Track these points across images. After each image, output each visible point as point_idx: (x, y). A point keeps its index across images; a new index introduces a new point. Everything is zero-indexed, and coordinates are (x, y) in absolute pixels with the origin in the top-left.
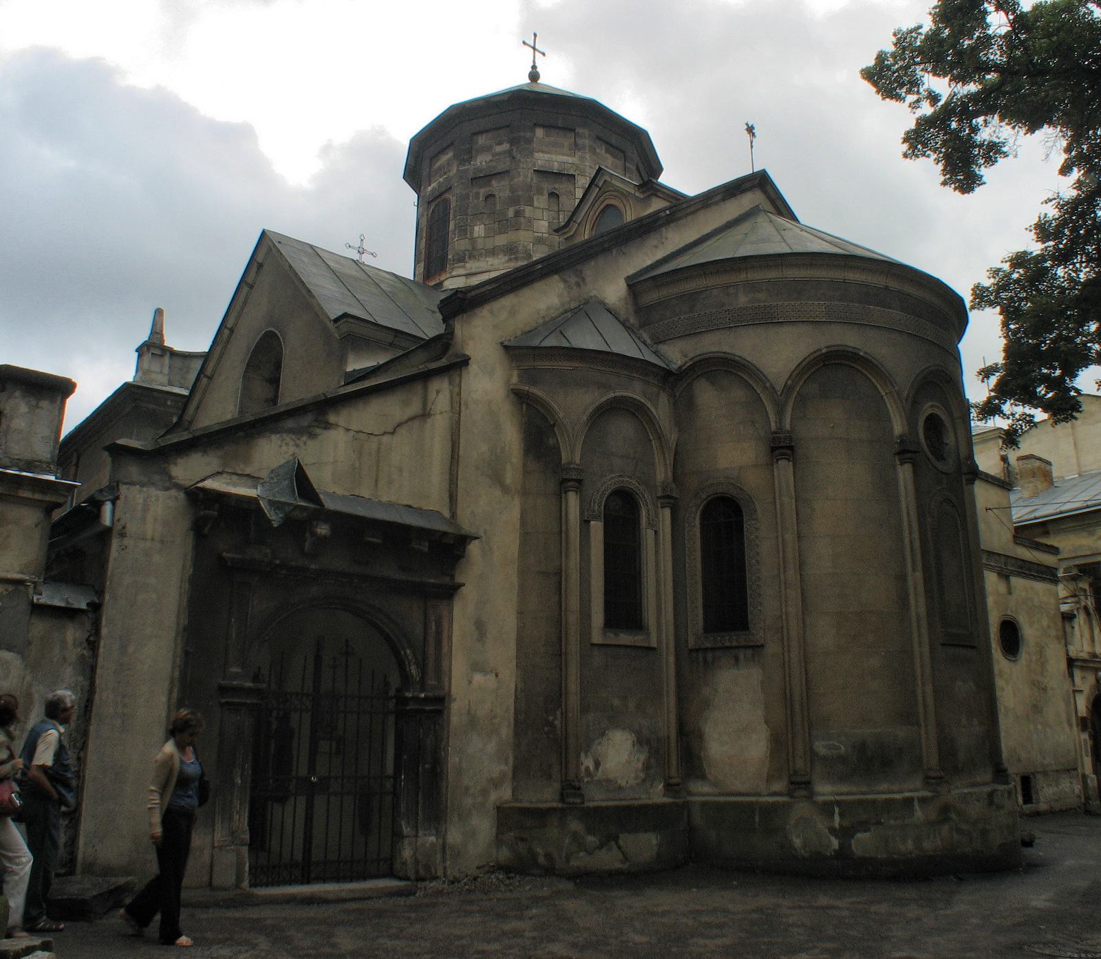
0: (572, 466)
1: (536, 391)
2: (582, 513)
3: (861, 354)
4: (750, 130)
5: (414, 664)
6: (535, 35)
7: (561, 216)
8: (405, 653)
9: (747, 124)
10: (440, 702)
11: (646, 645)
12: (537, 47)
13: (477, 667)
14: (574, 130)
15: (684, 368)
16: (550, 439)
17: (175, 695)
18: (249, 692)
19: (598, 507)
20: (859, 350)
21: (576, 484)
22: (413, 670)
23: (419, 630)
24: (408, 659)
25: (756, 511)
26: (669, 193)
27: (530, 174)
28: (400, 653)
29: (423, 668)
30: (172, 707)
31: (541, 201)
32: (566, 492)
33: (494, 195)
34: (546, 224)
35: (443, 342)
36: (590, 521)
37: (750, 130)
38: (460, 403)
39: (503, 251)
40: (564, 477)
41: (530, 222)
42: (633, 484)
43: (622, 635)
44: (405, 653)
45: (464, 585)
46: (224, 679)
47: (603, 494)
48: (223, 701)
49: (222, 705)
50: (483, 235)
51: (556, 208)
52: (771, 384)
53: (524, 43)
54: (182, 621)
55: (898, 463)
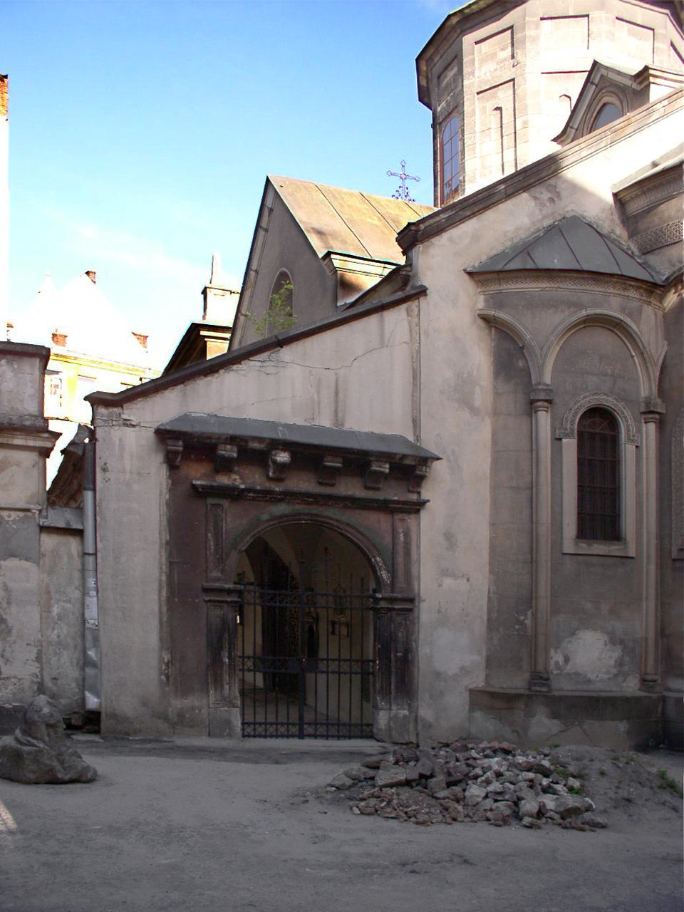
0: (540, 387)
2: (553, 429)
5: (384, 569)
8: (376, 560)
10: (408, 604)
11: (623, 555)
13: (445, 573)
17: (164, 593)
18: (229, 592)
21: (546, 404)
22: (384, 575)
23: (388, 540)
24: (378, 565)
28: (370, 560)
29: (393, 573)
30: (163, 603)
32: (536, 412)
36: (560, 439)
38: (420, 333)
40: (532, 398)
42: (609, 402)
43: (595, 545)
44: (375, 560)
45: (428, 501)
46: (206, 582)
47: (576, 413)
48: (207, 599)
49: (207, 602)
54: (164, 536)
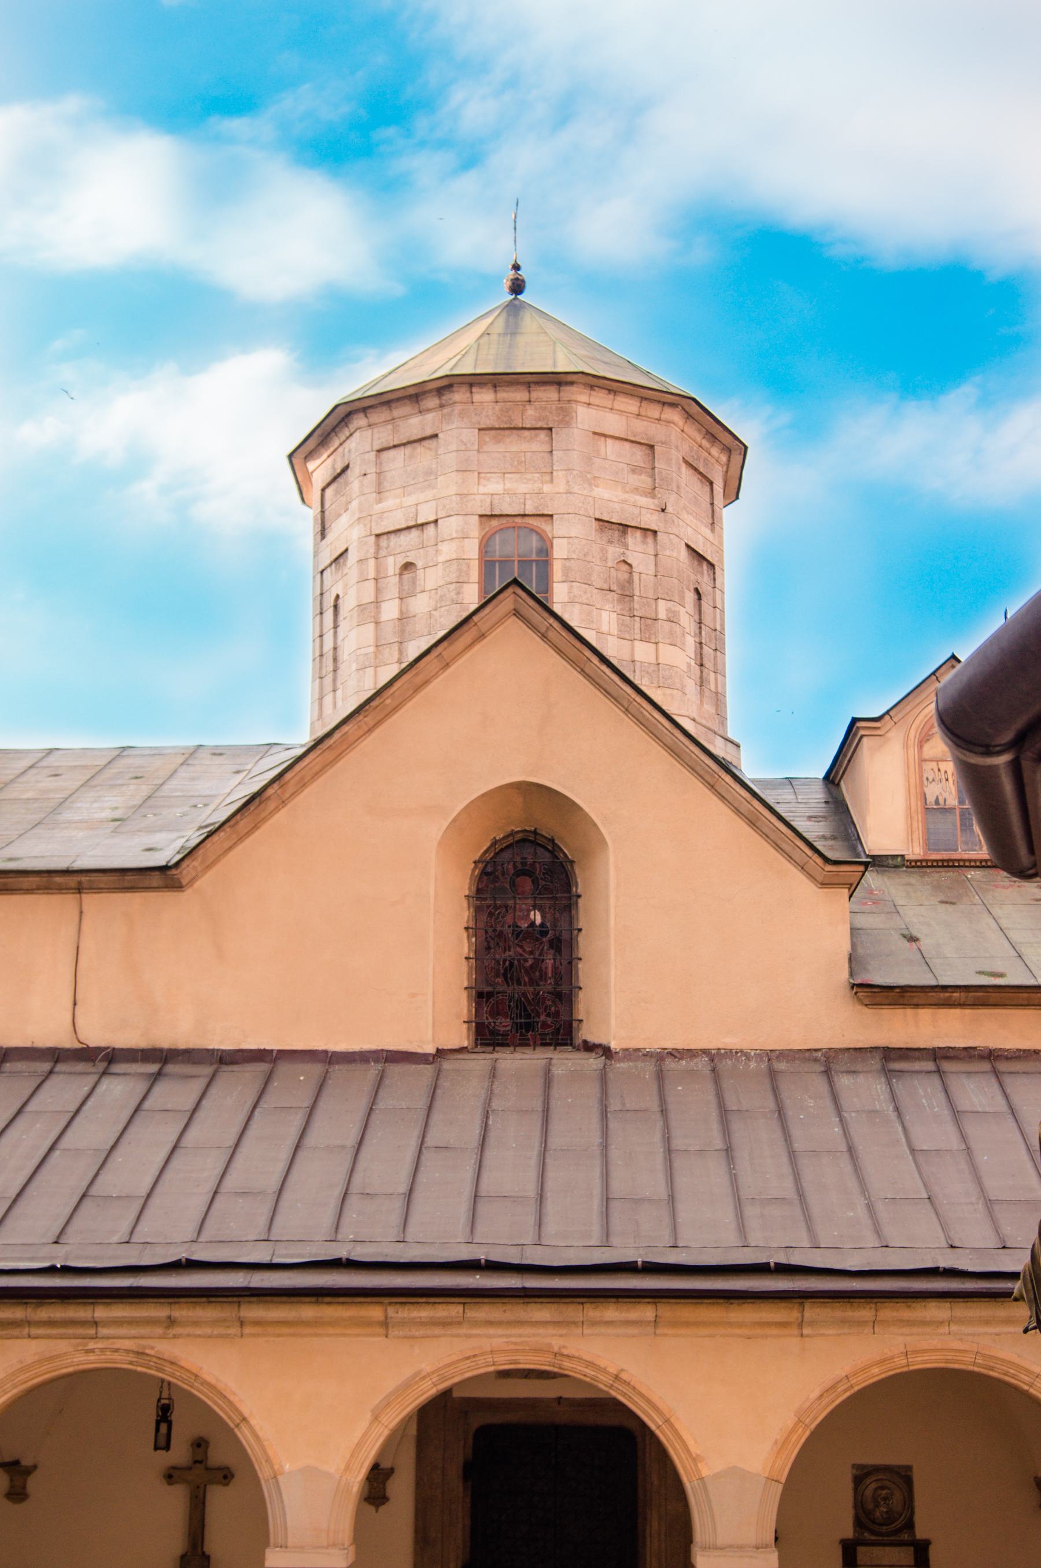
27: (684, 553)
33: (630, 565)
39: (648, 673)
41: (684, 635)
50: (616, 632)
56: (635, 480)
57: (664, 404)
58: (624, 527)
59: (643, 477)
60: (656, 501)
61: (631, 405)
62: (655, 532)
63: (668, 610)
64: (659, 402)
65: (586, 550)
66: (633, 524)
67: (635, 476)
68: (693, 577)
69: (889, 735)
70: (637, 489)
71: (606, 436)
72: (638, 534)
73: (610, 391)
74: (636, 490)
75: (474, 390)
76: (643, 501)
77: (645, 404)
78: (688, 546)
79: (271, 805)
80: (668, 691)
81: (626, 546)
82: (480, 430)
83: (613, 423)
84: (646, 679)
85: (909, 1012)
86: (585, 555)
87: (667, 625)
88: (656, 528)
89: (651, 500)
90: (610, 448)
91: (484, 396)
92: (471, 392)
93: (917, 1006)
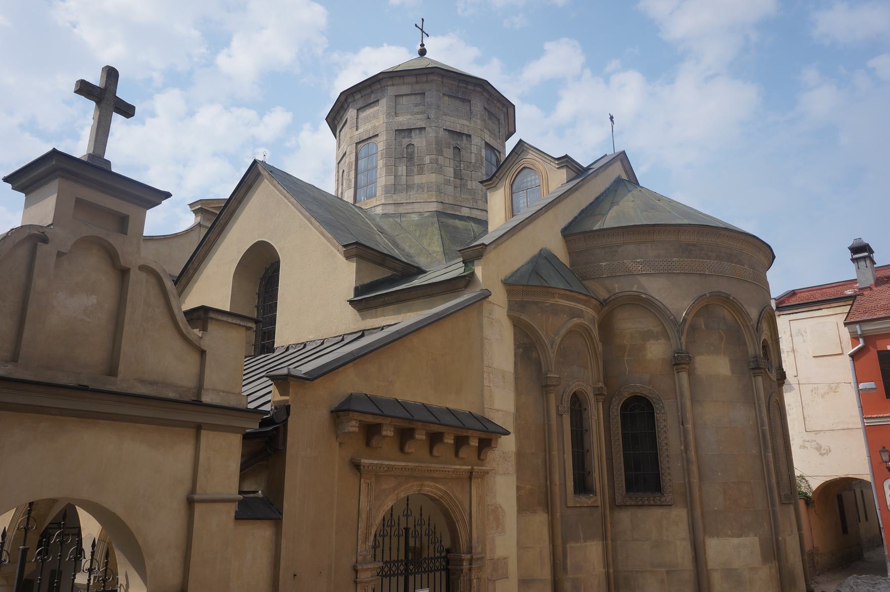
1: (524, 317)
2: (557, 407)
3: (731, 298)
4: (612, 118)
6: (423, 20)
7: (462, 165)
9: (610, 115)
12: (424, 29)
14: (470, 101)
15: (608, 302)
16: (534, 353)
19: (567, 404)
20: (730, 295)
25: (663, 408)
26: (578, 167)
27: (442, 133)
31: (449, 153)
32: (546, 394)
34: (452, 170)
35: (466, 281)
36: (562, 415)
37: (612, 118)
39: (421, 188)
41: (441, 168)
50: (405, 175)
51: (458, 159)
52: (674, 317)
53: (416, 25)
55: (752, 375)
56: (416, 109)
57: (427, 74)
58: (410, 130)
59: (421, 107)
60: (425, 115)
61: (413, 79)
62: (425, 128)
63: (431, 159)
64: (424, 74)
65: (390, 144)
66: (413, 128)
67: (417, 108)
68: (452, 142)
69: (497, 186)
70: (417, 113)
71: (402, 96)
72: (417, 131)
73: (400, 77)
74: (417, 113)
75: (354, 95)
76: (419, 116)
77: (418, 76)
78: (444, 129)
79: (191, 272)
80: (430, 193)
81: (411, 137)
82: (358, 110)
83: (405, 90)
84: (420, 190)
85: (374, 310)
86: (390, 146)
87: (430, 165)
88: (425, 126)
89: (423, 115)
90: (404, 100)
91: (358, 96)
92: (353, 96)
93: (376, 307)
